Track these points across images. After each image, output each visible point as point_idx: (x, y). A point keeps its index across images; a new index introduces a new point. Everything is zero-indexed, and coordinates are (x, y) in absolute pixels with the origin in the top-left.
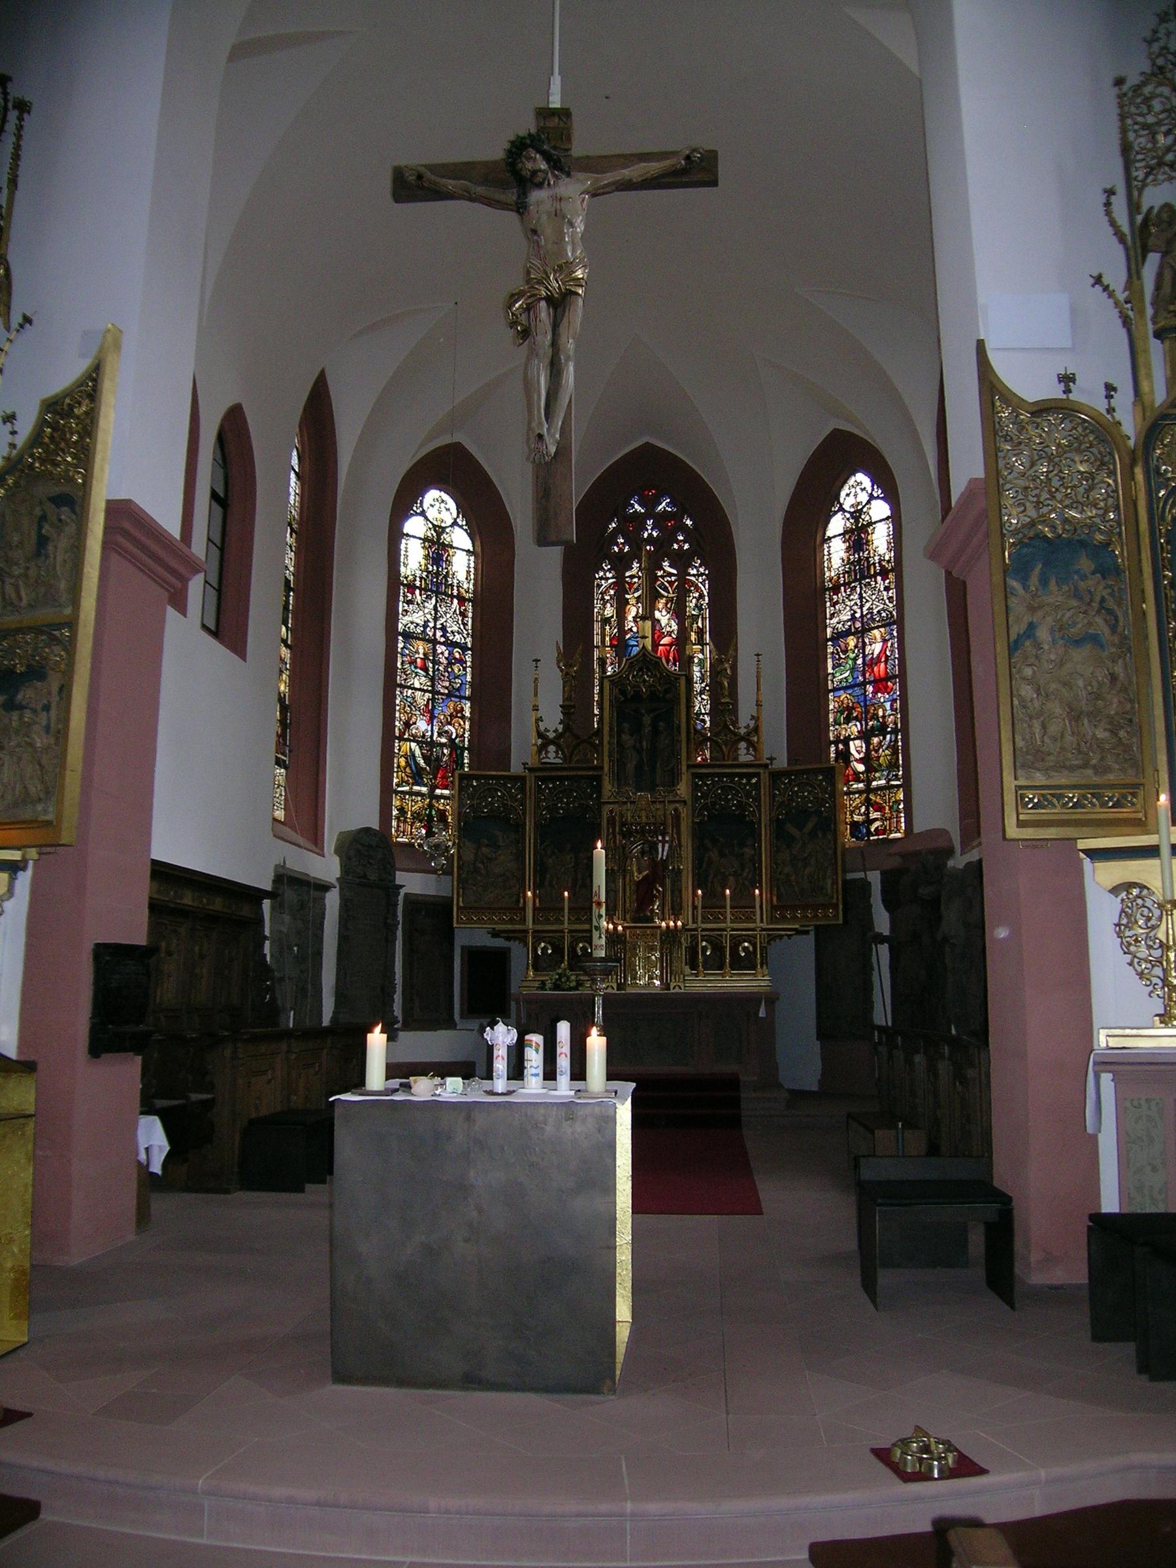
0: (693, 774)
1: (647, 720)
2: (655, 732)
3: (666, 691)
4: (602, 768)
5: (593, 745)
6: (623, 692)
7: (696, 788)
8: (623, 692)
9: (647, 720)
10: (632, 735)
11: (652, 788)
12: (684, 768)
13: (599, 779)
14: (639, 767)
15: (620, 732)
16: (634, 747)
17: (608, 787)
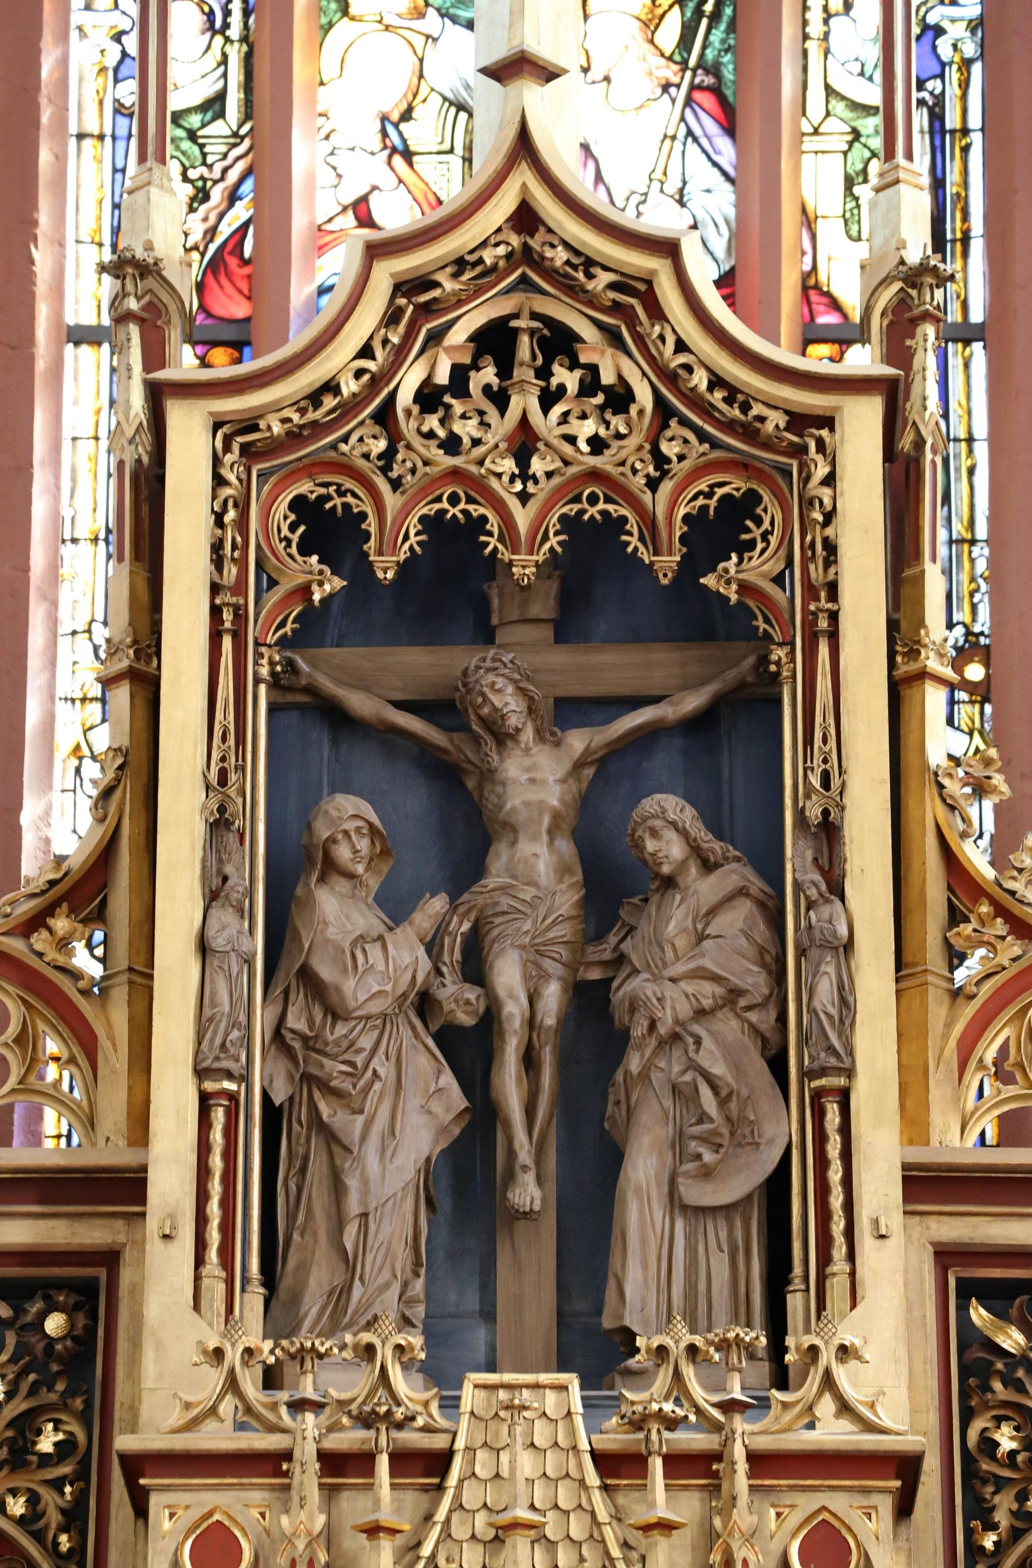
0: (946, 1256)
1: (536, 779)
2: (614, 885)
3: (722, 530)
4: (126, 1188)
5: (51, 995)
6: (326, 531)
7: (971, 1373)
8: (326, 531)
9: (536, 779)
10: (395, 907)
11: (597, 1352)
12: (879, 1188)
13: (92, 1287)
14: (466, 1177)
15: (296, 866)
16: (425, 1004)
17: (180, 1350)
